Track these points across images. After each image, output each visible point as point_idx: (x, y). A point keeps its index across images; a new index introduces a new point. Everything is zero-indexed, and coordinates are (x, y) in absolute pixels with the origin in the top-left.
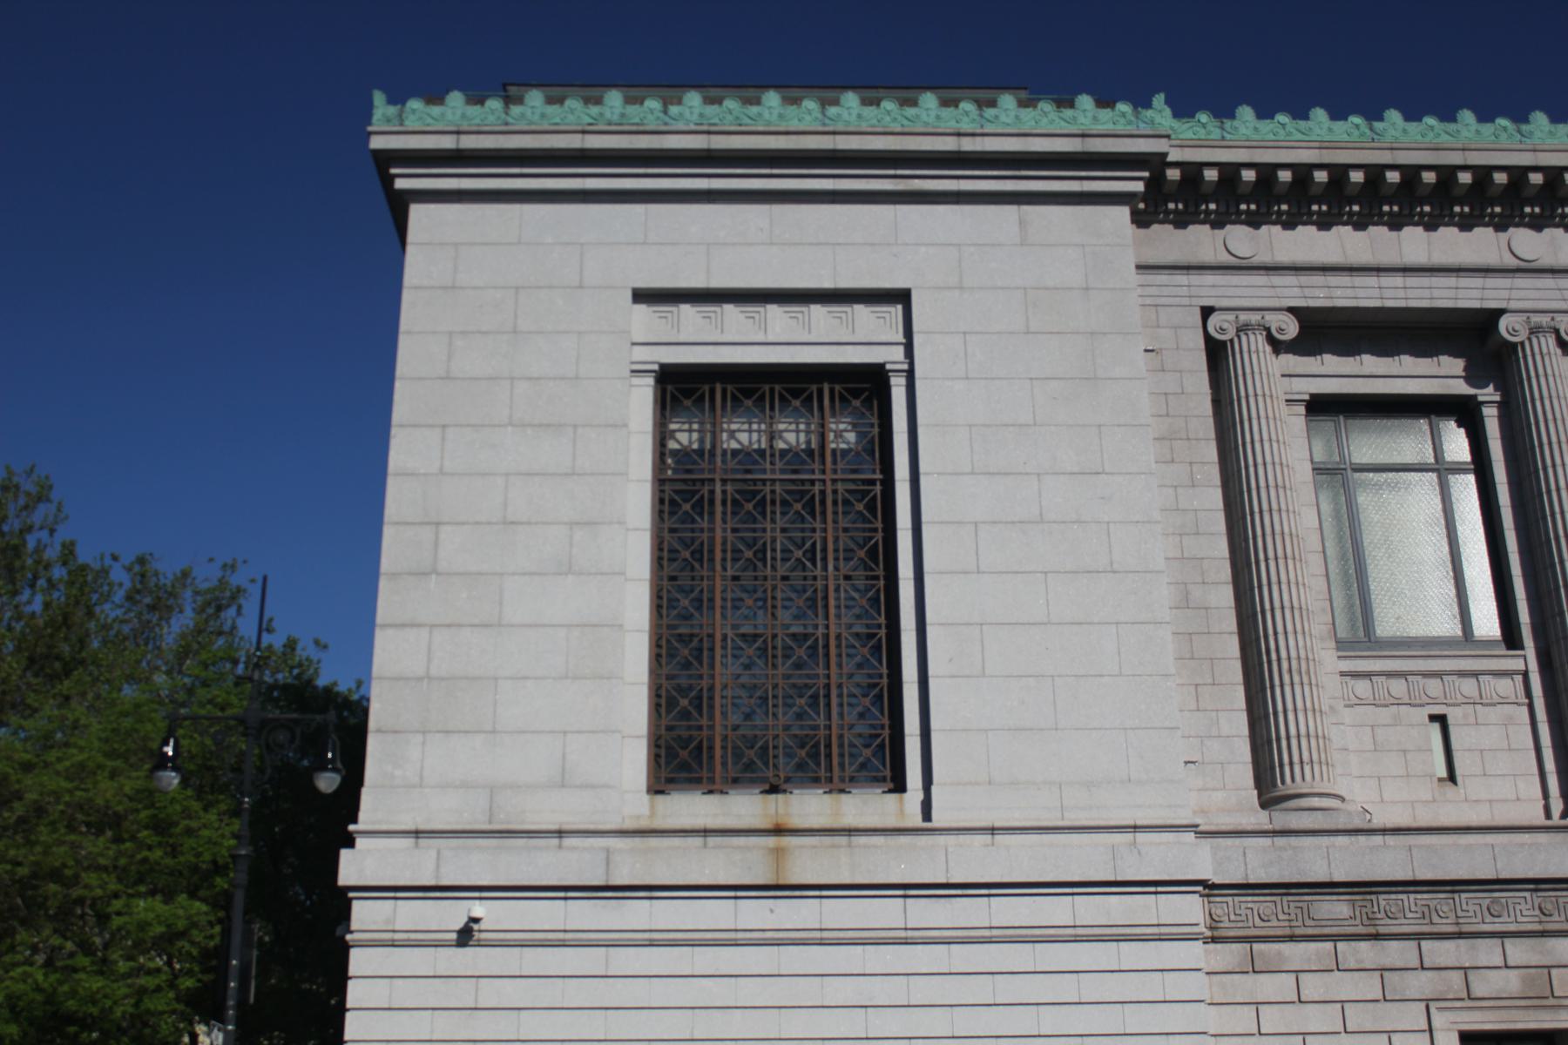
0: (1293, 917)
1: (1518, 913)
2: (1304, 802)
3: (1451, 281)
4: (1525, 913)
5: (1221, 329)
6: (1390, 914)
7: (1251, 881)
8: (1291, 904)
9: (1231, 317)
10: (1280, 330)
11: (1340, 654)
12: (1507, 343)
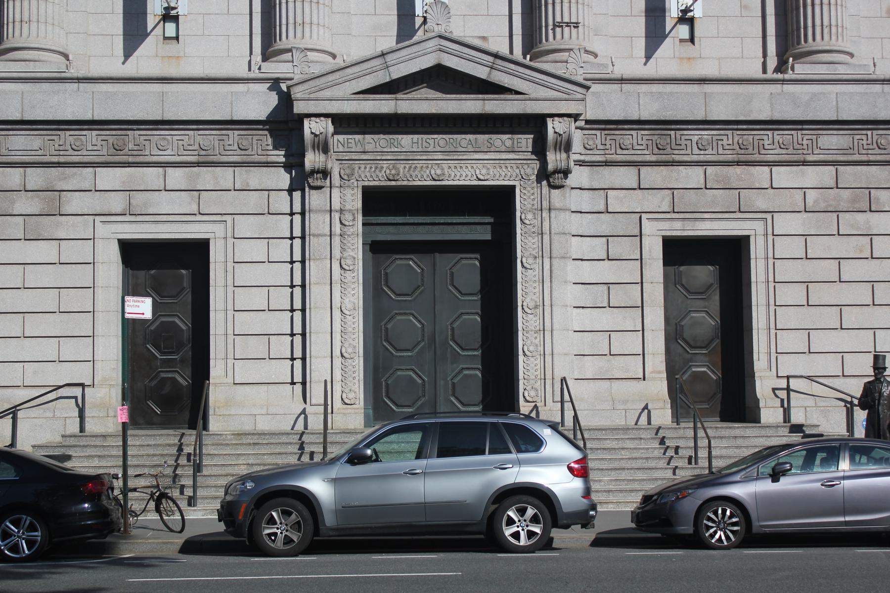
1: (761, 147)
2: (551, 57)
4: (766, 147)
6: (782, 146)
7: (235, 118)
8: (644, 137)
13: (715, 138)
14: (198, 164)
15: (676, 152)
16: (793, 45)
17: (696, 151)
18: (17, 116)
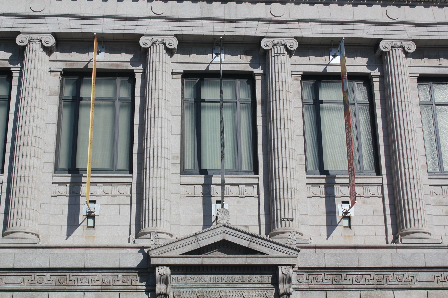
0: (310, 281)
1: (388, 280)
3: (135, 22)
4: (391, 280)
5: (21, 41)
6: (399, 280)
7: (121, 267)
9: (150, 38)
10: (46, 42)
11: (182, 176)
12: (383, 52)
13: (364, 276)
14: (101, 290)
15: (345, 283)
16: (400, 229)
17: (355, 283)
18: (11, 266)
